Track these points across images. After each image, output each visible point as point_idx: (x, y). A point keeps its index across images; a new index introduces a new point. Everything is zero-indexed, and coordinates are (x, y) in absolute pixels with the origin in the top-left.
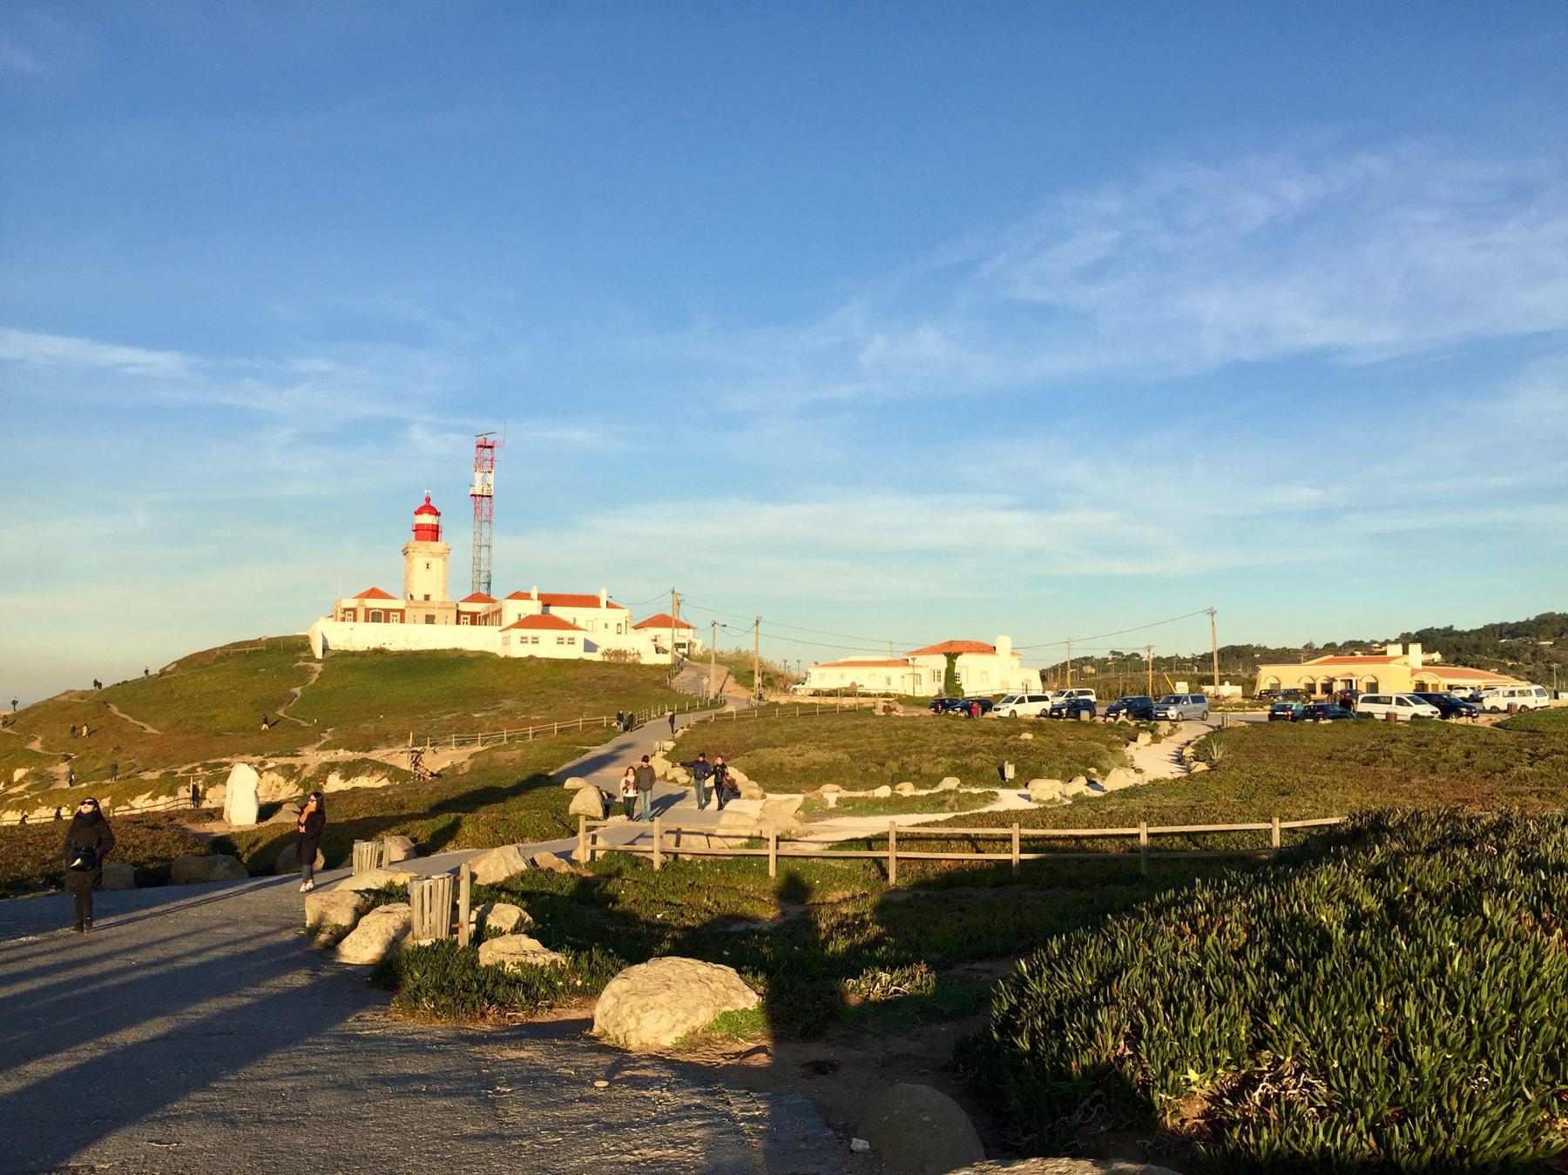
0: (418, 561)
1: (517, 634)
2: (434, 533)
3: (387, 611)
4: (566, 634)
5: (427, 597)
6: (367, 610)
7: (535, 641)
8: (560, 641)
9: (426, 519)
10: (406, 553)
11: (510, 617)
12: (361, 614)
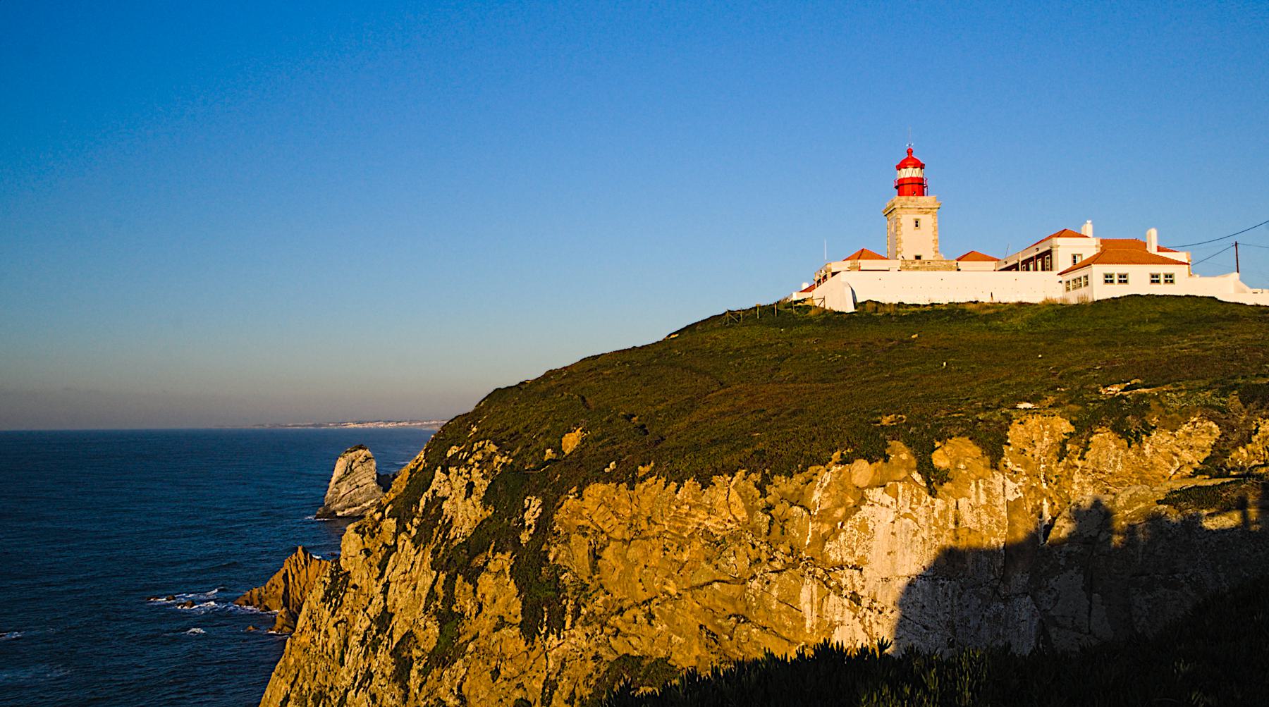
0: (906, 220)
1: (1098, 271)
2: (918, 187)
4: (1162, 270)
7: (1123, 279)
8: (1155, 279)
9: (910, 173)
10: (890, 212)
11: (1062, 260)
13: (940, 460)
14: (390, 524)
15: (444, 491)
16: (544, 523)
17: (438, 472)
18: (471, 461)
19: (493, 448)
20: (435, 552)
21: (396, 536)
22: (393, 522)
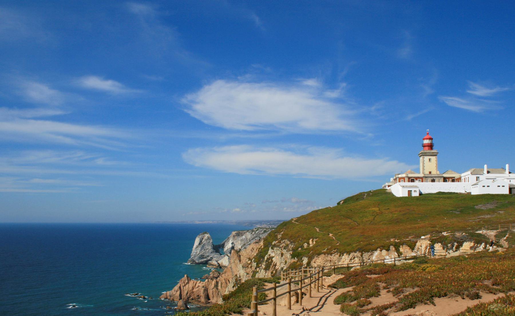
3: (417, 178)
5: (430, 173)
6: (409, 178)
12: (406, 179)
13: (401, 250)
14: (254, 264)
15: (273, 255)
16: (309, 264)
17: (270, 249)
18: (281, 246)
19: (289, 243)
20: (272, 273)
21: (256, 269)
22: (255, 263)
